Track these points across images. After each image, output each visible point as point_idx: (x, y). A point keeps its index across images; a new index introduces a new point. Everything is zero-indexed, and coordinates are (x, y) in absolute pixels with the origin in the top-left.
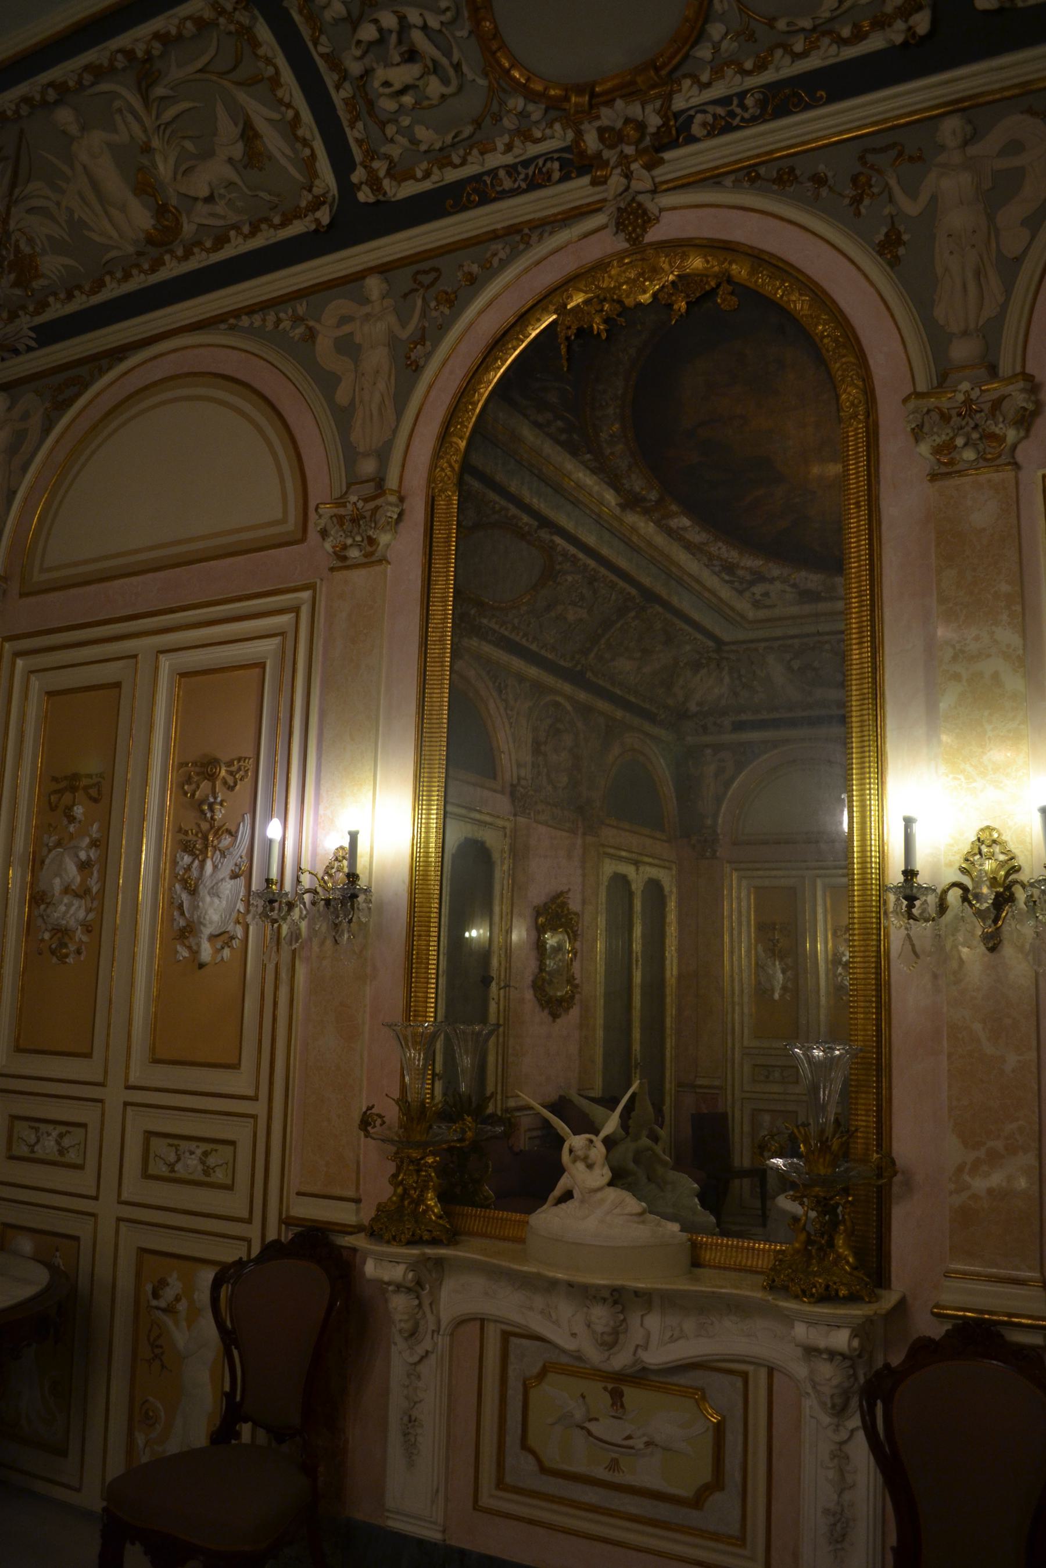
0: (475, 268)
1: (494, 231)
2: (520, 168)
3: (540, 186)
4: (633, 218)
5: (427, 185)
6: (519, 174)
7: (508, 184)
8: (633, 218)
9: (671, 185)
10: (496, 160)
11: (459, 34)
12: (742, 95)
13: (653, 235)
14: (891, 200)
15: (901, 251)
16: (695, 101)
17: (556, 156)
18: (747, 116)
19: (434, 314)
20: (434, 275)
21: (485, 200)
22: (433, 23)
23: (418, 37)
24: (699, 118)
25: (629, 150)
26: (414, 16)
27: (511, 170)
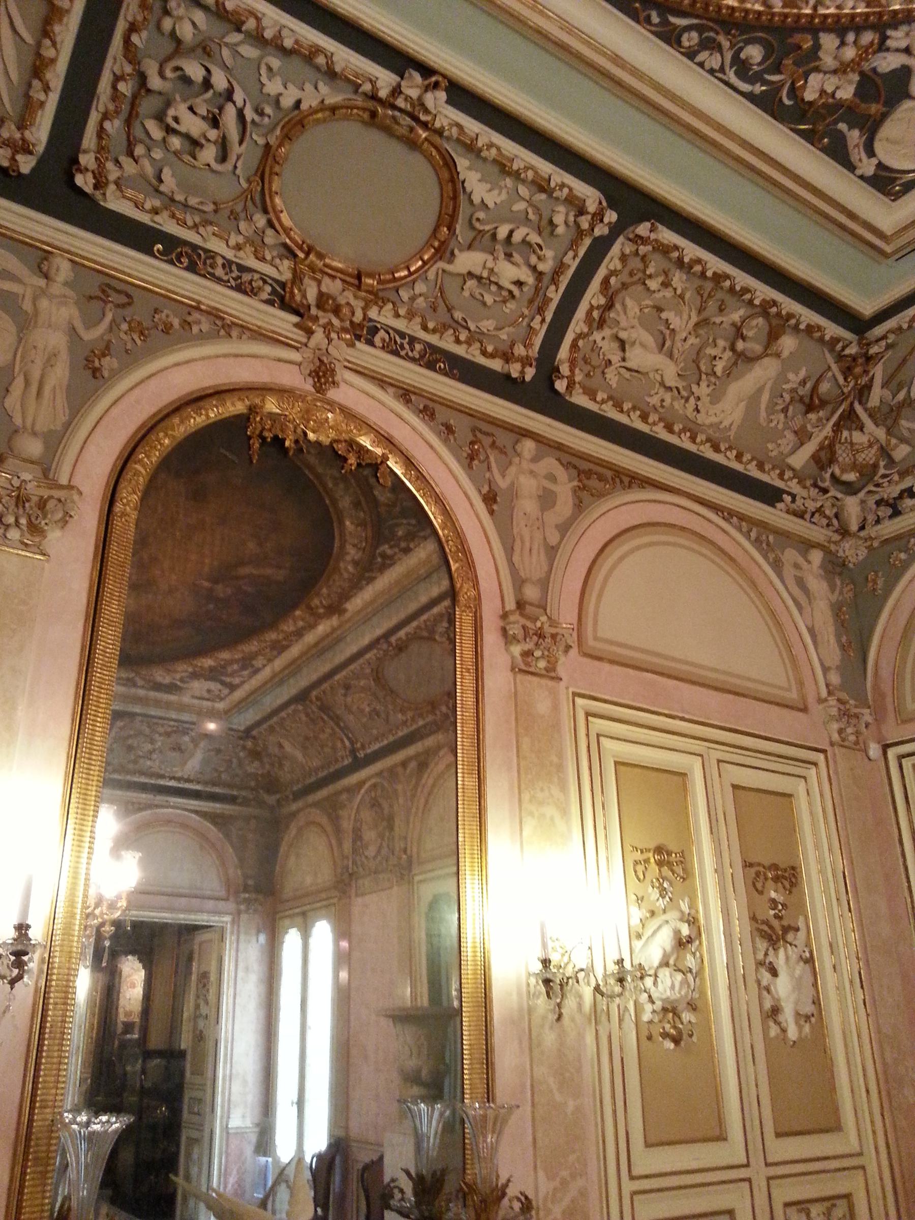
0: (176, 322)
1: (199, 302)
2: (234, 268)
3: (245, 293)
4: (323, 375)
5: (144, 218)
6: (231, 271)
7: (219, 272)
8: (323, 375)
9: (355, 367)
10: (215, 245)
11: (255, 137)
12: (413, 340)
13: (332, 394)
14: (489, 468)
15: (495, 507)
16: (382, 319)
17: (270, 281)
18: (410, 354)
19: (122, 335)
20: (123, 299)
21: (192, 268)
22: (249, 114)
23: (230, 113)
24: (382, 333)
25: (336, 322)
26: (239, 96)
27: (228, 264)
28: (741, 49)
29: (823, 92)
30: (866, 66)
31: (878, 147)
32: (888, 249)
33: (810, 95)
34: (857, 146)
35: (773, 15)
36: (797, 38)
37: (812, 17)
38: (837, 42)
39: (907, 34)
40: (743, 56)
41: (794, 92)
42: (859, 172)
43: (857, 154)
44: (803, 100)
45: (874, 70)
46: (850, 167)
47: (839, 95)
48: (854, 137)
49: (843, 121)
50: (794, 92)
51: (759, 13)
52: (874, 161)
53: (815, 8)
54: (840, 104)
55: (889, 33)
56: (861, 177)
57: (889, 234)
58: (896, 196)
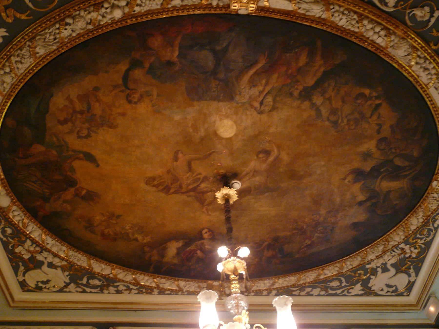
28: (6, 227)
29: (20, 252)
30: (34, 255)
31: (26, 275)
32: (12, 304)
33: (17, 250)
34: (21, 271)
35: (19, 227)
36: (22, 236)
37: (28, 234)
38: (31, 244)
39: (48, 255)
40: (6, 229)
41: (13, 247)
42: (18, 278)
43: (20, 273)
44: (14, 250)
45: (36, 257)
46: (17, 276)
47: (24, 256)
48: (22, 268)
49: (22, 263)
50: (13, 247)
51: (16, 224)
52: (23, 278)
53: (30, 233)
54: (23, 258)
55: (44, 251)
56: (18, 280)
57: (16, 300)
58: (24, 291)
